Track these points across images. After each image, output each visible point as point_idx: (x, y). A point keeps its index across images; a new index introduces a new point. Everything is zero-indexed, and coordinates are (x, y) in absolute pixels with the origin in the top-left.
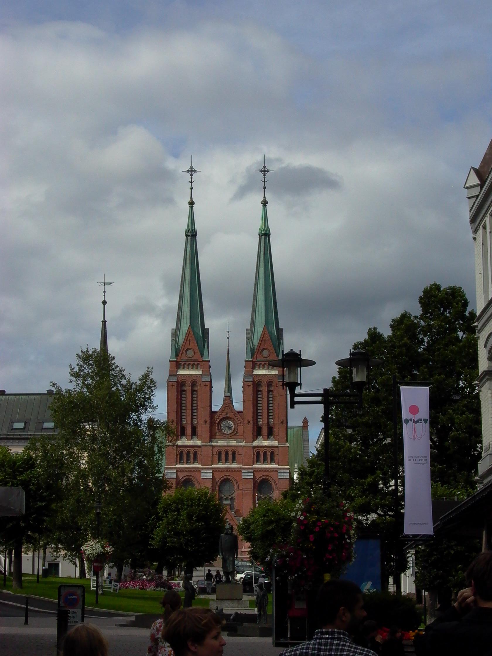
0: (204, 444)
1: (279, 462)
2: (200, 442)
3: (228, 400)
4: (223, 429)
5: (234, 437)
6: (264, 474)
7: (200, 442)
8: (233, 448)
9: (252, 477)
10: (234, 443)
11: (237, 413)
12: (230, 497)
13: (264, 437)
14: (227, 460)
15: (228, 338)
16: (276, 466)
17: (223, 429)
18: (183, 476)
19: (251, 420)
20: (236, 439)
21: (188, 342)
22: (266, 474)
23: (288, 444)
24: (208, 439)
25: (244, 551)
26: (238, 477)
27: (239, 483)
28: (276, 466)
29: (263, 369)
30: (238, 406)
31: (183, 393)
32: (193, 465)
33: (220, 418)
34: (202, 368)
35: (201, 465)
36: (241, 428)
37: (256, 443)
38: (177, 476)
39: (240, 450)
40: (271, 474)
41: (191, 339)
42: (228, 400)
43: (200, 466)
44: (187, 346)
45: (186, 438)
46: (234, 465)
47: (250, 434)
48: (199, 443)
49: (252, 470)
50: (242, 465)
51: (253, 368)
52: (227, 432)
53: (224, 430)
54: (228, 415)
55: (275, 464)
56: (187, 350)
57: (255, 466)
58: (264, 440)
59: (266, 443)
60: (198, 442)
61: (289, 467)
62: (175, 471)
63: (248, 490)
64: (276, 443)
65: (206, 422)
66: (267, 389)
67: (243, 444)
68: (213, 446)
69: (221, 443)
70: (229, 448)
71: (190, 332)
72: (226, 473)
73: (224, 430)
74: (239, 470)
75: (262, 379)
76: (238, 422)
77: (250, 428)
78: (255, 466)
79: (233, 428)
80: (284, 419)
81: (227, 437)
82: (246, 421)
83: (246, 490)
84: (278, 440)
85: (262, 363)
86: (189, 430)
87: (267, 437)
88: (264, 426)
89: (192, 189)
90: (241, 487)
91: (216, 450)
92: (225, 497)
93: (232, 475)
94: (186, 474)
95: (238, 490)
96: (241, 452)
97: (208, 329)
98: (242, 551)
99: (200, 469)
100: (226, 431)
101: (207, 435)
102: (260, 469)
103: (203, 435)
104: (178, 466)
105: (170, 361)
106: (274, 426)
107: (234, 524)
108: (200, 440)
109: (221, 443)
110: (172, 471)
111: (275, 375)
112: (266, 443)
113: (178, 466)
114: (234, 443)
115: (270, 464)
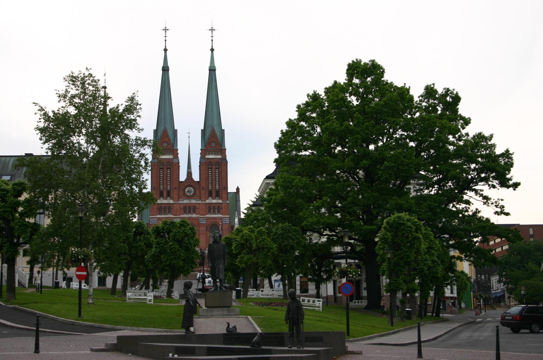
0: (175, 202)
2: (172, 201)
3: (189, 174)
6: (213, 221)
8: (193, 205)
9: (205, 223)
10: (194, 201)
15: (189, 137)
16: (221, 216)
20: (195, 199)
23: (228, 202)
28: (221, 216)
29: (212, 154)
30: (196, 177)
33: (185, 185)
34: (173, 154)
36: (198, 192)
37: (207, 201)
39: (198, 206)
42: (189, 174)
43: (172, 216)
45: (163, 198)
46: (194, 216)
48: (171, 202)
49: (205, 219)
51: (206, 154)
54: (189, 184)
56: (163, 142)
57: (207, 216)
59: (214, 201)
61: (228, 216)
62: (156, 219)
64: (220, 201)
65: (176, 188)
67: (200, 202)
69: (186, 201)
74: (197, 219)
76: (196, 188)
77: (203, 192)
78: (207, 216)
81: (189, 197)
82: (201, 188)
84: (222, 199)
86: (165, 194)
89: (166, 40)
91: (182, 206)
96: (198, 207)
97: (177, 130)
101: (176, 196)
104: (158, 216)
109: (186, 201)
110: (154, 219)
111: (220, 158)
112: (214, 201)
113: (158, 216)
114: (194, 201)
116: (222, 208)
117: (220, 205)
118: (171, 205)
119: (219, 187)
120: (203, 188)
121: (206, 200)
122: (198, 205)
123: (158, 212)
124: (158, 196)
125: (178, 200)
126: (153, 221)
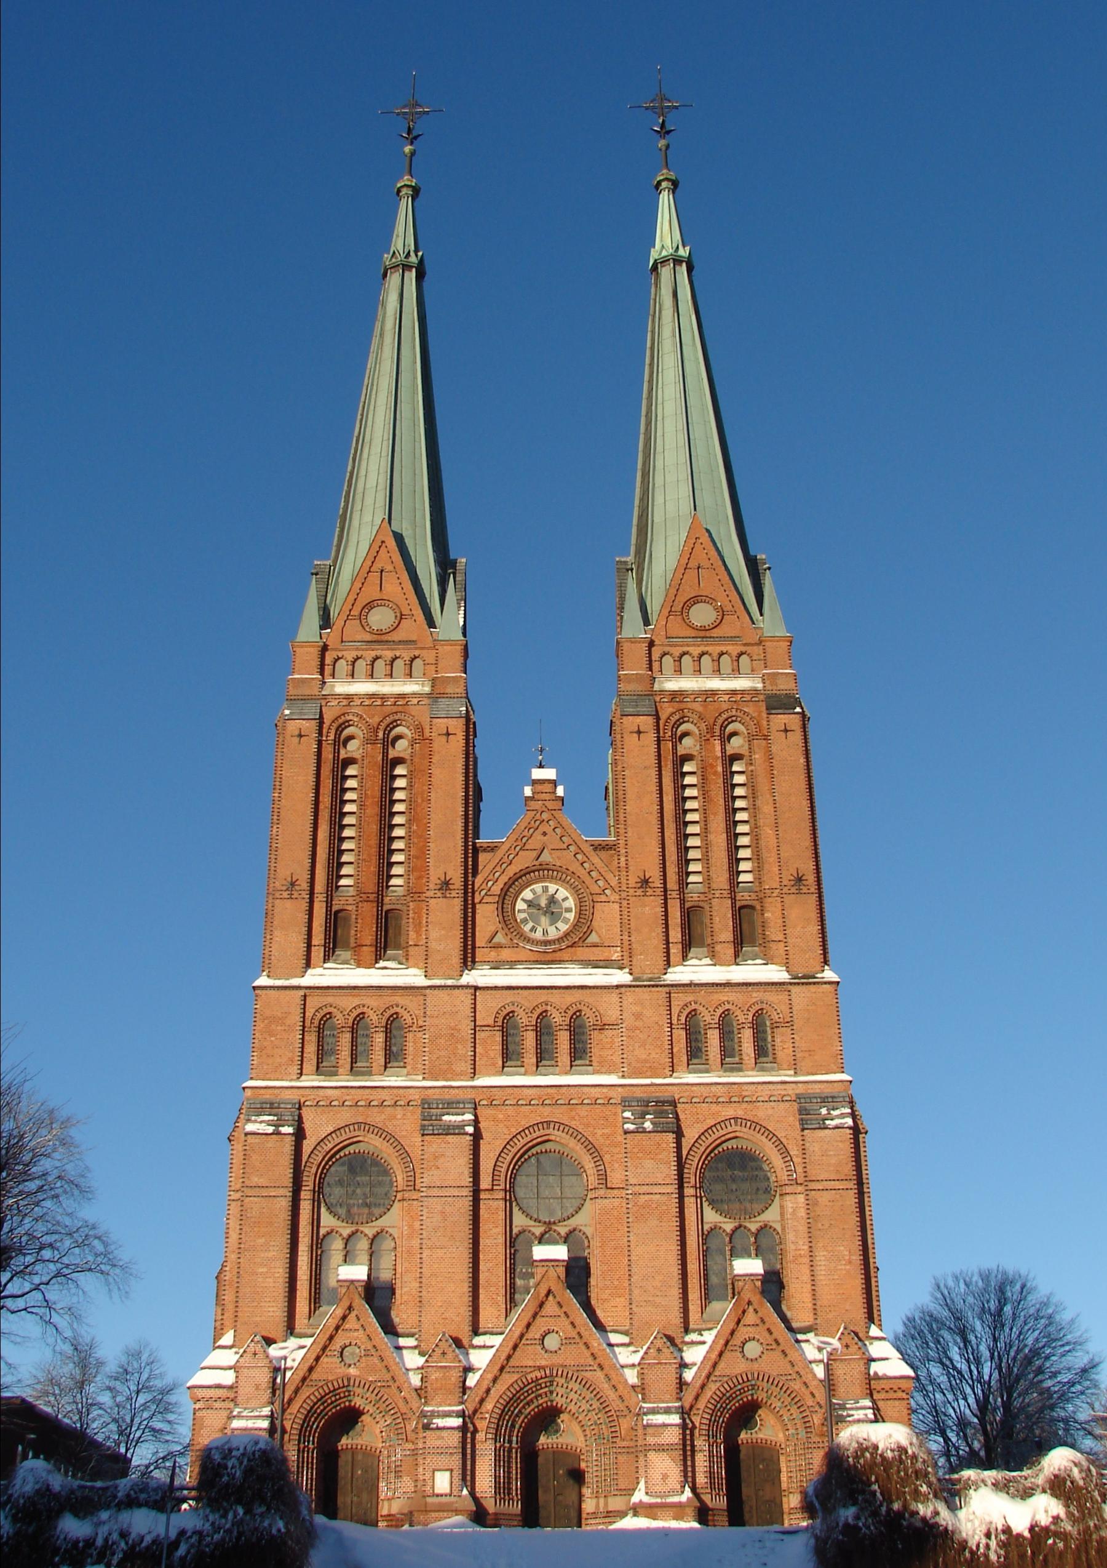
4: (525, 921)
5: (582, 953)
6: (729, 1112)
8: (570, 998)
11: (588, 849)
12: (563, 1230)
13: (718, 948)
14: (544, 1056)
17: (525, 921)
19: (655, 875)
21: (374, 577)
22: (740, 1113)
24: (456, 959)
26: (599, 1132)
36: (607, 918)
41: (389, 567)
44: (371, 592)
47: (650, 940)
48: (413, 977)
52: (545, 932)
53: (530, 924)
54: (546, 857)
56: (370, 606)
63: (656, 1189)
66: (718, 748)
68: (476, 988)
70: (555, 998)
71: (383, 542)
73: (530, 924)
79: (571, 916)
80: (807, 868)
82: (633, 881)
83: (645, 1189)
87: (731, 951)
88: (715, 902)
90: (616, 1177)
92: (538, 1231)
94: (346, 1116)
96: (611, 1014)
100: (540, 930)
103: (433, 945)
106: (761, 900)
107: (590, 1361)
116: (790, 1023)
119: (759, 880)
120: (645, 882)
122: (614, 997)
123: (311, 1048)
125: (469, 959)
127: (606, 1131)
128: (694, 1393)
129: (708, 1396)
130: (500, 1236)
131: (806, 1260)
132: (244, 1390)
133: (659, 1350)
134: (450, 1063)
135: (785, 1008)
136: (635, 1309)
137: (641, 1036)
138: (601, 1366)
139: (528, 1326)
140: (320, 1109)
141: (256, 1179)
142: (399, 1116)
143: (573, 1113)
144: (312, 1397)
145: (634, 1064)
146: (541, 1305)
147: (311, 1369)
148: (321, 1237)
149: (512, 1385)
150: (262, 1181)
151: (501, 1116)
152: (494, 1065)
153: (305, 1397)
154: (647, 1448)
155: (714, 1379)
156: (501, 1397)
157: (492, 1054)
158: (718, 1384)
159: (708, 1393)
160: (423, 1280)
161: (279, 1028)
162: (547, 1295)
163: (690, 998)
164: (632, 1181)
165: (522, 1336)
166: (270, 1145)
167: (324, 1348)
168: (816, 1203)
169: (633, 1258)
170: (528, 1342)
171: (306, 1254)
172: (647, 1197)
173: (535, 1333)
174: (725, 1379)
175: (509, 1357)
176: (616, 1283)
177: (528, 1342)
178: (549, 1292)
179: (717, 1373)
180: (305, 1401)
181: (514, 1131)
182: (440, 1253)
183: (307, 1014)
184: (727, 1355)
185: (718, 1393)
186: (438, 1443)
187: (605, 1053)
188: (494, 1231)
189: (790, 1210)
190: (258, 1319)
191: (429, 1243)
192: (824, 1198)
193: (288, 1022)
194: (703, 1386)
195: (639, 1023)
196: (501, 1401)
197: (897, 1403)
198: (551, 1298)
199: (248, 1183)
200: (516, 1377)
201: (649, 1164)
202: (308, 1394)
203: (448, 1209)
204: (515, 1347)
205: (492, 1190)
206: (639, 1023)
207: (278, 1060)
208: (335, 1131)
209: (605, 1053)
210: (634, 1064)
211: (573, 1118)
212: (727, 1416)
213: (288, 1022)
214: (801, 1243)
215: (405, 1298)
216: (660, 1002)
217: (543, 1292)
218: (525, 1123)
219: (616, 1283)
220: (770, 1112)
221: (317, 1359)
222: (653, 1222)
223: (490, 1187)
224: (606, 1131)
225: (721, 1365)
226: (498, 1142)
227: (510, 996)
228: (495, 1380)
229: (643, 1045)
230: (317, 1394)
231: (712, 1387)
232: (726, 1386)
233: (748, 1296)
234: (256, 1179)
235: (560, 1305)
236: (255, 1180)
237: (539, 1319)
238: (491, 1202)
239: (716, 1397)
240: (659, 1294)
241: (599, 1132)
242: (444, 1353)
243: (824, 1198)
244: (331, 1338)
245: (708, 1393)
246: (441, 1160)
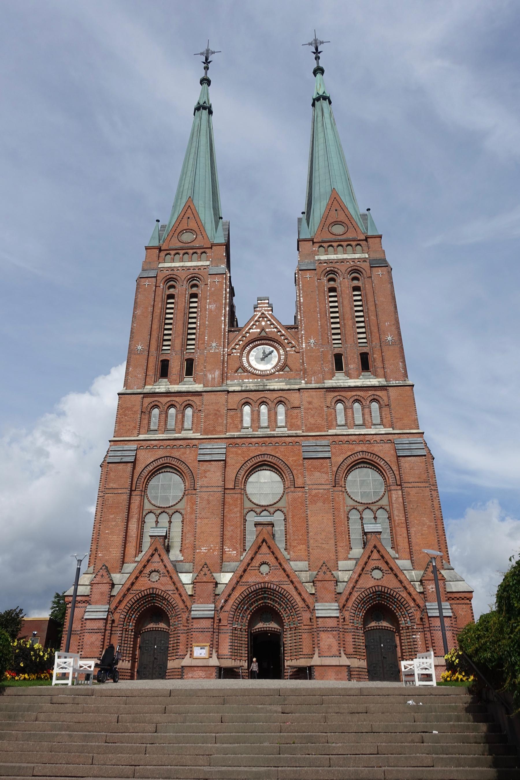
1: (394, 420)
2: (202, 385)
6: (359, 448)
7: (202, 385)
8: (275, 395)
18: (153, 460)
21: (185, 220)
22: (365, 449)
25: (319, 663)
26: (291, 459)
27: (295, 472)
31: (169, 301)
32: (180, 435)
35: (199, 434)
38: (135, 459)
40: (376, 449)
49: (324, 442)
50: (301, 432)
55: (384, 428)
58: (351, 378)
60: (196, 385)
63: (321, 487)
70: (268, 395)
72: (263, 449)
75: (336, 265)
83: (315, 486)
85: (333, 244)
90: (299, 482)
93: (277, 455)
94: (161, 453)
95: (293, 489)
98: (312, 663)
99: (195, 442)
102: (346, 438)
105: (147, 248)
107: (286, 579)
108: (200, 383)
110: (126, 447)
115: (371, 428)
117: (378, 393)
118: (195, 399)
121: (325, 381)
122: (297, 395)
124: (151, 373)
126: (119, 453)
127: (294, 458)
128: (345, 598)
129: (354, 598)
130: (238, 513)
131: (404, 525)
132: (95, 597)
133: (325, 573)
134: (214, 427)
135: (386, 398)
136: (311, 551)
137: (312, 412)
138: (292, 582)
139: (252, 559)
140: (148, 450)
141: (112, 485)
142: (187, 453)
143: (277, 450)
144: (133, 600)
145: (308, 426)
146: (259, 547)
147: (133, 584)
148: (144, 514)
149: (242, 592)
150: (115, 486)
151: (240, 452)
152: (237, 427)
153: (128, 600)
154: (319, 630)
155: (356, 590)
156: (236, 599)
157: (236, 422)
158: (359, 593)
159: (353, 598)
160: (197, 535)
161: (130, 412)
162: (262, 543)
163: (336, 394)
164: (309, 483)
165: (248, 564)
166: (120, 468)
167: (141, 572)
168: (409, 494)
169: (310, 523)
170: (252, 568)
171: (136, 523)
172: (316, 491)
173: (256, 563)
174: (363, 590)
175: (241, 577)
176: (301, 537)
177: (252, 568)
178: (264, 541)
179: (358, 586)
180: (128, 602)
181: (246, 459)
182: (206, 521)
183: (144, 406)
184: (363, 576)
185: (359, 598)
186: (199, 626)
187: (293, 421)
188: (235, 510)
189: (394, 499)
190: (107, 558)
191: (201, 516)
192: (413, 492)
193: (134, 409)
194: (350, 594)
195: (311, 406)
196: (237, 602)
197: (464, 606)
198: (264, 543)
199: (107, 487)
200: (246, 587)
201: (317, 474)
202: (130, 598)
203: (211, 498)
204: (245, 571)
205: (234, 489)
206: (311, 406)
207: (129, 427)
208: (154, 461)
209: (293, 421)
210: (308, 426)
211: (277, 452)
212: (365, 612)
213: (134, 409)
214: (401, 516)
215: (187, 545)
216: (321, 396)
217: (260, 541)
218: (252, 455)
219: (301, 537)
220: (381, 448)
221: (137, 578)
222: (320, 504)
223: (233, 487)
224: (294, 458)
225: (360, 582)
226: (238, 465)
227: (245, 395)
228: (234, 589)
229: (313, 416)
230: (135, 598)
231: (355, 595)
232: (363, 594)
233: (374, 543)
234: (112, 485)
235: (269, 547)
236: (112, 485)
237: (258, 556)
238: (234, 495)
239: (358, 600)
240: (324, 542)
241: (291, 459)
242: (205, 574)
243: (413, 492)
244: (145, 566)
245: (353, 598)
246: (208, 473)
